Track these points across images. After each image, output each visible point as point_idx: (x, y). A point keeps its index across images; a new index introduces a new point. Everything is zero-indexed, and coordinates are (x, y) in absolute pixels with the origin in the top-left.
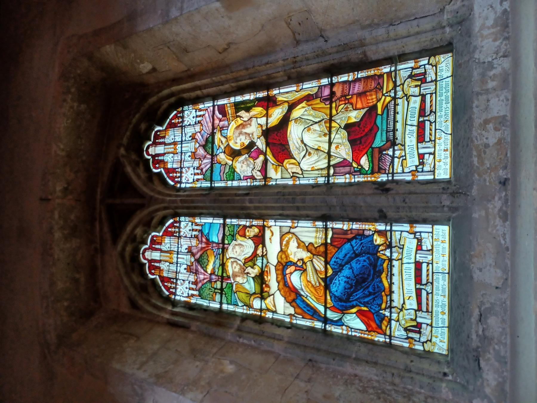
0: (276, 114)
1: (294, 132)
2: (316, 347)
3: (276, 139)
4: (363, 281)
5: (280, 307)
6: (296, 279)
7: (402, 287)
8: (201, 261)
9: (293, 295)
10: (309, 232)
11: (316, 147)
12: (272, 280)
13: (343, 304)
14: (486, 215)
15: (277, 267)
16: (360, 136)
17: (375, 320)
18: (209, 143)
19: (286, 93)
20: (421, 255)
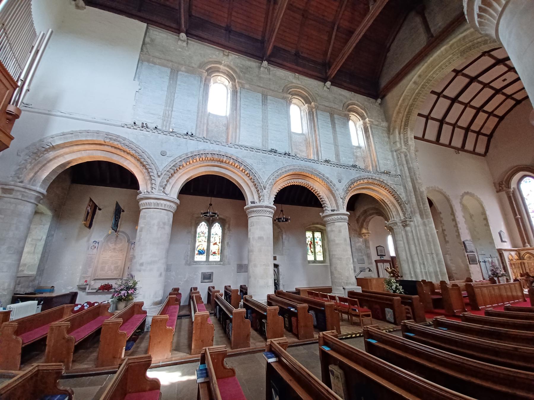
0: (218, 243)
1: (216, 245)
2: (194, 249)
3: (215, 244)
4: (201, 253)
5: (197, 244)
6: (201, 246)
7: (201, 256)
8: (202, 233)
9: (199, 246)
10: (205, 248)
11: (214, 248)
12: (200, 243)
13: (199, 251)
14: (207, 263)
15: (201, 243)
16: (214, 253)
17: (197, 254)
18: (216, 234)
19: (220, 245)
20: (203, 258)
